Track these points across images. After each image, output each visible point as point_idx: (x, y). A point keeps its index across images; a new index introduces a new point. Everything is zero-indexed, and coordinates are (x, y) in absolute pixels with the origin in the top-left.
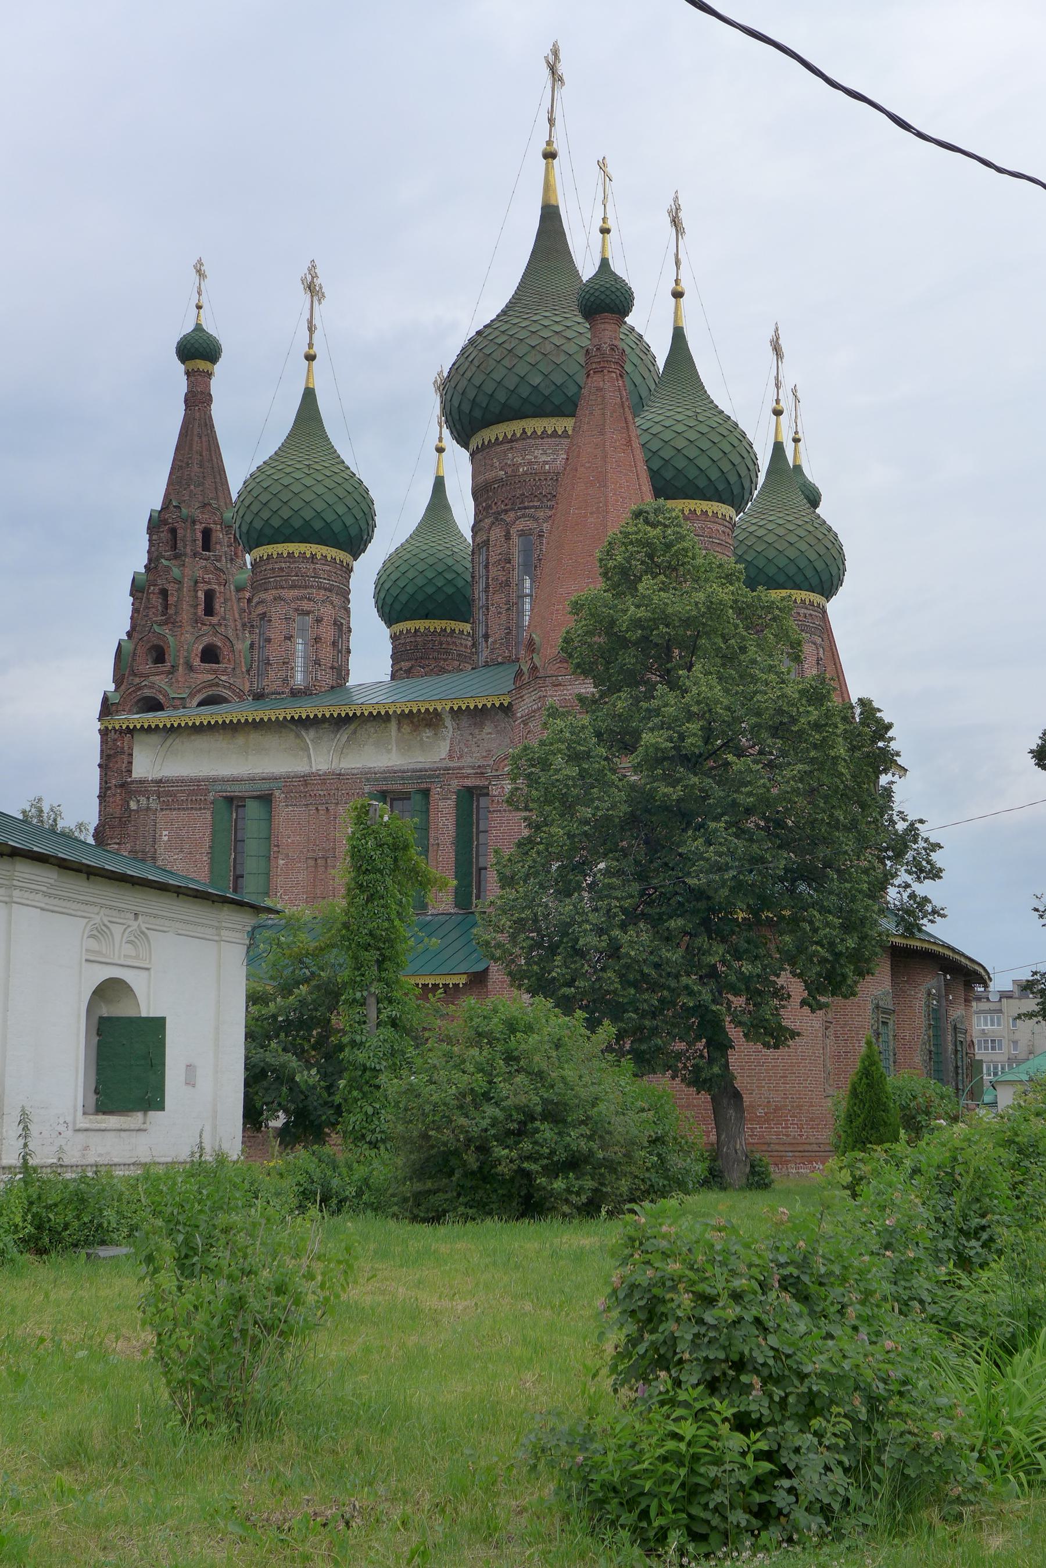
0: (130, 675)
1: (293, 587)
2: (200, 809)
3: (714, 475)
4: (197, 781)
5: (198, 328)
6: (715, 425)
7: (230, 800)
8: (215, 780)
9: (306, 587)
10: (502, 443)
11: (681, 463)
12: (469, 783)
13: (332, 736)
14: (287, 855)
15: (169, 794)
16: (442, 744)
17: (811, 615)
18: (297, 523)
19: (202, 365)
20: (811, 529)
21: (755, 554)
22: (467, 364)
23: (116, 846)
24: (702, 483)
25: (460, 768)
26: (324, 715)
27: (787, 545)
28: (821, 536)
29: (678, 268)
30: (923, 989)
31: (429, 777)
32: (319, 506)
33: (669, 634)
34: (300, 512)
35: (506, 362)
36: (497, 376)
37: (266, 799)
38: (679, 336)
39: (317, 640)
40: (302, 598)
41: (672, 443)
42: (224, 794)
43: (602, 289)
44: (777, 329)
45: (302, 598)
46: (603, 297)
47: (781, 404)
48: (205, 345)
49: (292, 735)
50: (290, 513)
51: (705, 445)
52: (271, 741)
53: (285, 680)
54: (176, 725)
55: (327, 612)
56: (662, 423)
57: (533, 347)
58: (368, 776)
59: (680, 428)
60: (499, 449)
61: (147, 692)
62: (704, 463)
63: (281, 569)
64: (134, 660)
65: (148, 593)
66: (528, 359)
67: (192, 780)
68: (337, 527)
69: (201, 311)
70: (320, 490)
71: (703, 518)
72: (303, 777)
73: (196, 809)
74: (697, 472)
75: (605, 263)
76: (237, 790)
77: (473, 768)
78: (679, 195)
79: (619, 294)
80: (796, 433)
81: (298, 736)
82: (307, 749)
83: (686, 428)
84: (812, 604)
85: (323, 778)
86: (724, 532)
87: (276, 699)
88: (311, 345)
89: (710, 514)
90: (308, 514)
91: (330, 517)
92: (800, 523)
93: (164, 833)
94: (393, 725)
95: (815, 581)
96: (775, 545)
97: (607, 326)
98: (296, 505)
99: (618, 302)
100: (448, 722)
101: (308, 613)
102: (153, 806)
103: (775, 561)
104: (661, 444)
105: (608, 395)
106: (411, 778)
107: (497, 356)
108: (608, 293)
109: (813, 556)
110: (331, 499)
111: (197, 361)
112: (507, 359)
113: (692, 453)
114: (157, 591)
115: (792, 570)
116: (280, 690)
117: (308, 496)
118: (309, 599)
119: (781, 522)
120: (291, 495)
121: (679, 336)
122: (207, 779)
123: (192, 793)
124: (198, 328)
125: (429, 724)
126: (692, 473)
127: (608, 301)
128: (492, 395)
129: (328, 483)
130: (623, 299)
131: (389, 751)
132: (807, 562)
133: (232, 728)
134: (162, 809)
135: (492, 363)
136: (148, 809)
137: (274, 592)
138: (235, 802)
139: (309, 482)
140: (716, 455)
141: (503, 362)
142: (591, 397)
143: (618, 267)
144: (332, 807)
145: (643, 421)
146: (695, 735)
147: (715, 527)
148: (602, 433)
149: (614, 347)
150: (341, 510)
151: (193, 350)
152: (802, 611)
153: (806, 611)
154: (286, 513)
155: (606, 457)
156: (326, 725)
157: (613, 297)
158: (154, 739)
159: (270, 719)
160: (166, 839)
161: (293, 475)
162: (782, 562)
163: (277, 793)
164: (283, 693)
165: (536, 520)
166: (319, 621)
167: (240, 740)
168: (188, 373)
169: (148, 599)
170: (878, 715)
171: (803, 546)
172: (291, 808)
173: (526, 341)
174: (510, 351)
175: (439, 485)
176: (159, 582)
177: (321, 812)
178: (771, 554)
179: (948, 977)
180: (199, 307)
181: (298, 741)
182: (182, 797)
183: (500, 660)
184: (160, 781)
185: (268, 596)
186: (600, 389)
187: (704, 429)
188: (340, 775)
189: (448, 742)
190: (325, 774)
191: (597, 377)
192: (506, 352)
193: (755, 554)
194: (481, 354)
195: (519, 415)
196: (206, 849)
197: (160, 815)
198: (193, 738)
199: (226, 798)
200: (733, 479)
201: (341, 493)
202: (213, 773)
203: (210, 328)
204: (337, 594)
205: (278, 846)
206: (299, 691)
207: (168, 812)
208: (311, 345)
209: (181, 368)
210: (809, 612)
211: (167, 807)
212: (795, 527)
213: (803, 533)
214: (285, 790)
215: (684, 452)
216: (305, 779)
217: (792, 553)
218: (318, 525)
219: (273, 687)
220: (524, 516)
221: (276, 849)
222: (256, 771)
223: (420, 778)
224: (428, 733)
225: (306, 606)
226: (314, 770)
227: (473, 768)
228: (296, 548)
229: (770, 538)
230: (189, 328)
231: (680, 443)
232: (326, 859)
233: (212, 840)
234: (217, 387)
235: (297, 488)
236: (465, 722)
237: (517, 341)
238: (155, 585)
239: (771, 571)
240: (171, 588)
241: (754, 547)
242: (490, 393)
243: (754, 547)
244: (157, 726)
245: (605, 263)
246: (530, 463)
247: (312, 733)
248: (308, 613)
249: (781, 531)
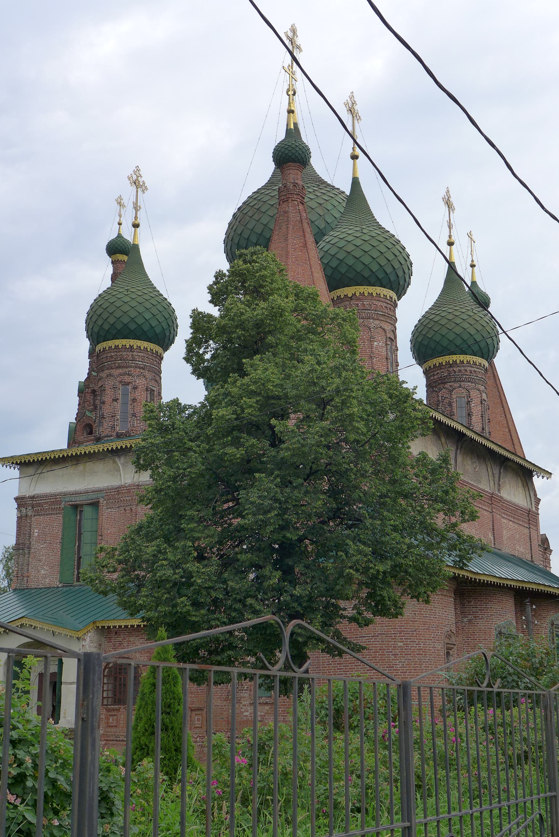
0: (73, 443)
1: (119, 367)
2: (57, 514)
3: (375, 268)
4: (55, 495)
5: (119, 236)
6: (375, 235)
7: (75, 507)
8: (65, 494)
9: (127, 367)
11: (351, 261)
15: (39, 505)
17: (475, 371)
18: (119, 326)
20: (471, 314)
21: (433, 333)
22: (237, 223)
24: (366, 274)
26: (126, 446)
27: (455, 325)
28: (478, 319)
30: (548, 621)
32: (133, 314)
33: (244, 336)
34: (121, 319)
35: (256, 217)
36: (250, 226)
37: (95, 504)
38: (355, 183)
39: (134, 400)
40: (124, 374)
41: (344, 249)
42: (71, 503)
43: (286, 147)
44: (448, 191)
45: (124, 374)
46: (287, 152)
47: (453, 238)
49: (111, 462)
51: (367, 248)
52: (98, 466)
53: (113, 427)
54: (36, 460)
55: (141, 382)
56: (345, 239)
57: (272, 205)
59: (350, 238)
62: (366, 260)
63: (111, 357)
64: (75, 433)
65: (85, 393)
66: (268, 213)
68: (146, 327)
69: (121, 226)
70: (134, 304)
71: (370, 298)
72: (116, 489)
73: (54, 514)
74: (363, 266)
76: (78, 500)
78: (354, 94)
79: (297, 149)
80: (472, 261)
81: (115, 462)
82: (119, 470)
83: (354, 238)
84: (475, 363)
86: (386, 307)
87: (107, 440)
88: (136, 218)
89: (375, 295)
90: (125, 320)
91: (140, 321)
92: (463, 310)
93: (36, 531)
95: (475, 348)
96: (447, 326)
97: (291, 171)
98: (118, 314)
99: (297, 155)
101: (128, 384)
102: (29, 513)
103: (447, 336)
104: (337, 250)
105: (291, 215)
107: (250, 214)
108: (290, 149)
109: (473, 332)
110: (141, 309)
111: (118, 255)
112: (256, 215)
113: (358, 254)
114: (90, 391)
115: (459, 342)
116: (109, 434)
117: (126, 308)
118: (129, 375)
119: (450, 311)
120: (115, 308)
121: (355, 183)
122: (60, 494)
123: (53, 503)
124: (119, 236)
126: (359, 267)
127: (290, 154)
128: (248, 239)
129: (140, 300)
130: (301, 152)
132: (469, 336)
134: (34, 515)
135: (247, 218)
136: (26, 516)
137: (107, 371)
138: (79, 509)
139: (126, 299)
140: (375, 254)
141: (254, 217)
142: (281, 218)
144: (134, 507)
145: (332, 238)
146: (251, 406)
147: (379, 304)
148: (286, 240)
149: (295, 185)
150: (148, 316)
152: (469, 369)
153: (471, 369)
154: (112, 320)
155: (288, 255)
157: (294, 151)
159: (94, 451)
160: (36, 534)
161: (117, 296)
162: (451, 336)
163: (101, 500)
164: (111, 436)
166: (135, 388)
167: (81, 467)
168: (113, 262)
169: (85, 396)
170: (404, 386)
171: (466, 325)
172: (110, 510)
173: (268, 202)
174: (258, 209)
177: (128, 511)
178: (444, 331)
179: (534, 607)
180: (120, 224)
182: (46, 507)
184: (33, 497)
185: (103, 374)
186: (286, 212)
187: (367, 238)
188: (138, 485)
190: (129, 486)
191: (284, 205)
192: (255, 211)
193: (433, 333)
194: (241, 214)
197: (33, 519)
199: (72, 505)
200: (389, 270)
201: (148, 305)
202: (65, 490)
204: (149, 371)
205: (101, 536)
206: (122, 434)
207: (38, 517)
208: (136, 218)
209: (109, 260)
210: (473, 369)
211: (37, 514)
212: (460, 313)
213: (465, 317)
214: (107, 498)
215: (353, 253)
216: (118, 490)
217: (458, 330)
218: (133, 326)
219: (106, 432)
221: (100, 538)
222: (90, 487)
225: (127, 379)
226: (123, 484)
228: (120, 342)
229: (443, 322)
230: (114, 236)
231: (350, 248)
233: (63, 535)
235: (118, 304)
237: (262, 203)
238: (89, 388)
239: (445, 343)
241: (433, 328)
242: (247, 237)
243: (433, 328)
244: (29, 461)
247: (123, 459)
248: (128, 384)
249: (450, 317)
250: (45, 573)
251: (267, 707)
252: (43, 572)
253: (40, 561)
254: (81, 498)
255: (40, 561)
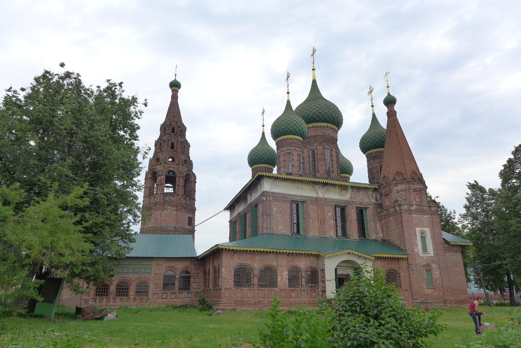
5: (175, 80)
8: (290, 195)
10: (321, 127)
12: (358, 206)
13: (322, 188)
14: (312, 219)
16: (348, 195)
19: (176, 88)
23: (161, 211)
25: (356, 202)
29: (372, 101)
31: (348, 203)
48: (176, 83)
50: (287, 129)
52: (305, 187)
58: (333, 200)
60: (320, 128)
61: (172, 169)
67: (283, 194)
75: (389, 94)
77: (359, 202)
85: (322, 199)
94: (337, 188)
100: (350, 190)
106: (343, 202)
124: (175, 80)
125: (344, 190)
131: (337, 195)
133: (294, 181)
137: (293, 148)
143: (391, 94)
151: (175, 84)
156: (321, 185)
158: (271, 180)
160: (275, 210)
165: (331, 147)
167: (296, 185)
175: (263, 134)
176: (172, 140)
181: (313, 188)
183: (323, 177)
184: (273, 193)
189: (350, 194)
195: (327, 122)
196: (288, 214)
198: (282, 182)
202: (289, 193)
203: (177, 80)
211: (274, 200)
216: (317, 199)
220: (328, 145)
223: (346, 203)
224: (344, 192)
227: (359, 202)
232: (324, 221)
234: (179, 95)
236: (355, 190)
240: (175, 143)
245: (389, 94)
246: (328, 133)
250: (282, 228)
251: (433, 290)
252: (280, 227)
253: (278, 222)
254: (297, 198)
255: (278, 222)
